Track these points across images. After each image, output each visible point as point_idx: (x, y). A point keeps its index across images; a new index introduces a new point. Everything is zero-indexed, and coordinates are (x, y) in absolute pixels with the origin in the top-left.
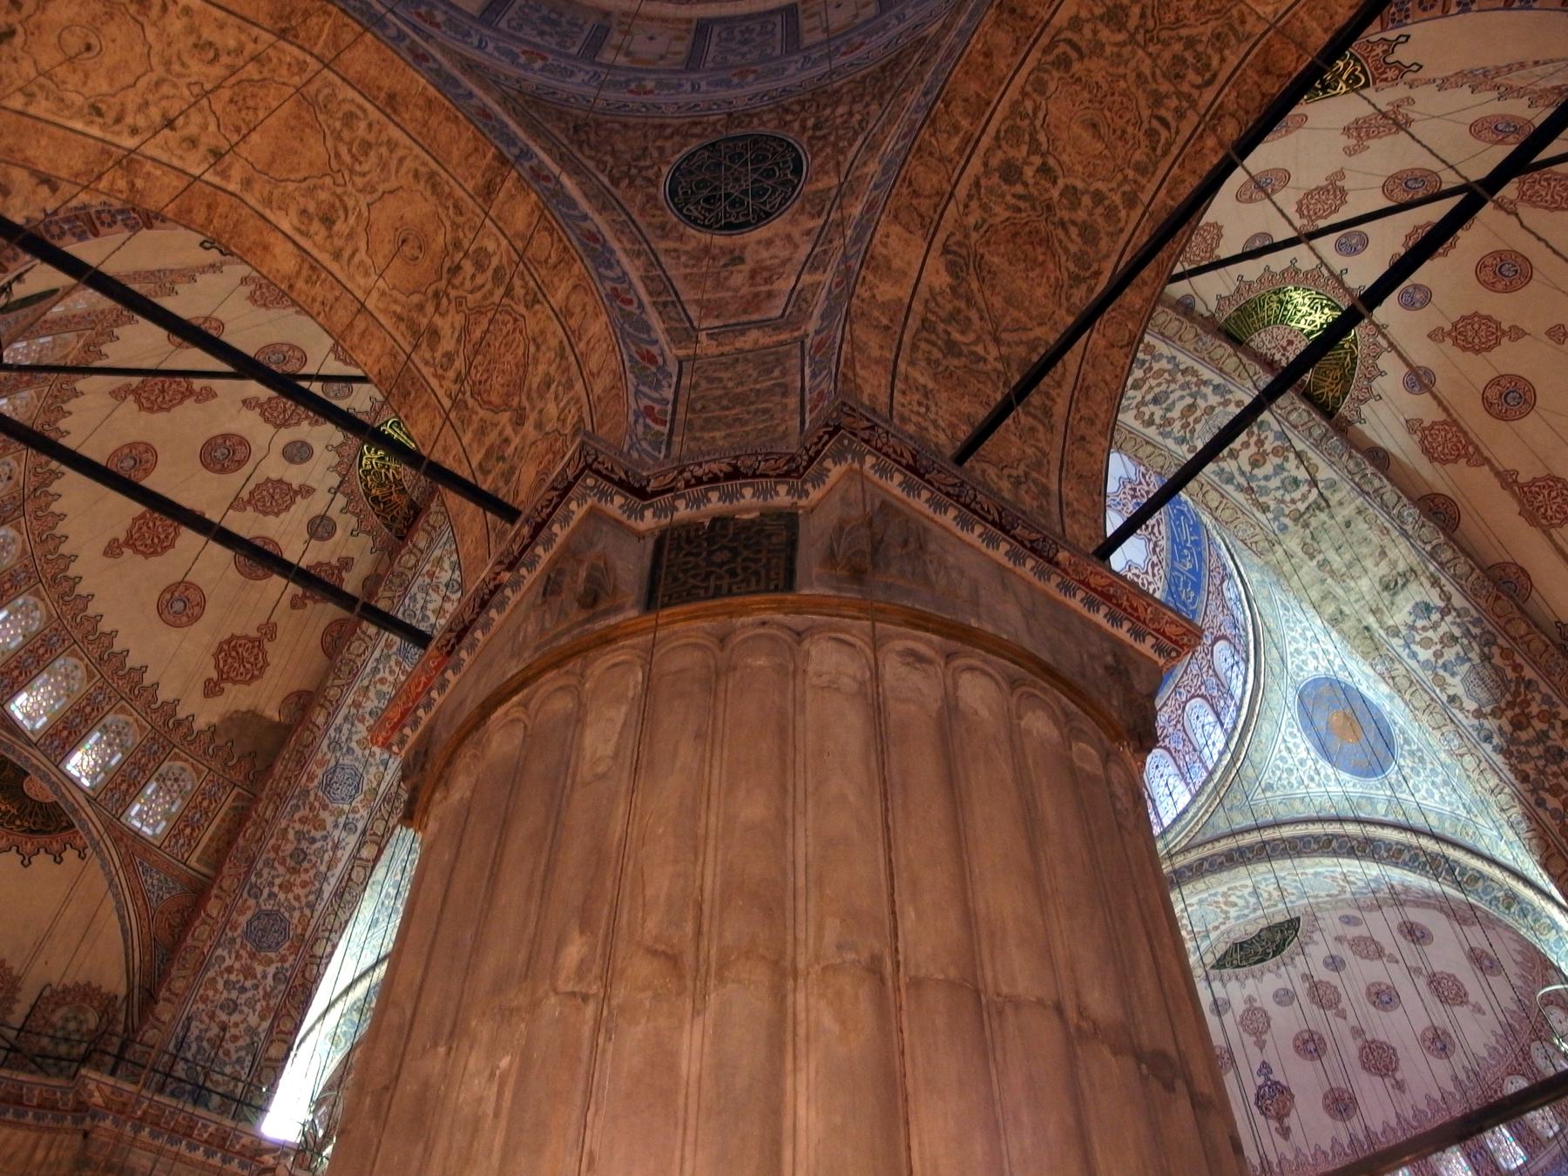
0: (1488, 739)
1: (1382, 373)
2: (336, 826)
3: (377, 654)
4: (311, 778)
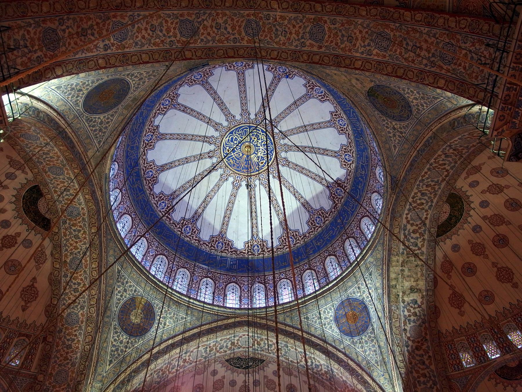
0: (407, 346)
1: (451, 239)
2: (103, 41)
3: (175, 12)
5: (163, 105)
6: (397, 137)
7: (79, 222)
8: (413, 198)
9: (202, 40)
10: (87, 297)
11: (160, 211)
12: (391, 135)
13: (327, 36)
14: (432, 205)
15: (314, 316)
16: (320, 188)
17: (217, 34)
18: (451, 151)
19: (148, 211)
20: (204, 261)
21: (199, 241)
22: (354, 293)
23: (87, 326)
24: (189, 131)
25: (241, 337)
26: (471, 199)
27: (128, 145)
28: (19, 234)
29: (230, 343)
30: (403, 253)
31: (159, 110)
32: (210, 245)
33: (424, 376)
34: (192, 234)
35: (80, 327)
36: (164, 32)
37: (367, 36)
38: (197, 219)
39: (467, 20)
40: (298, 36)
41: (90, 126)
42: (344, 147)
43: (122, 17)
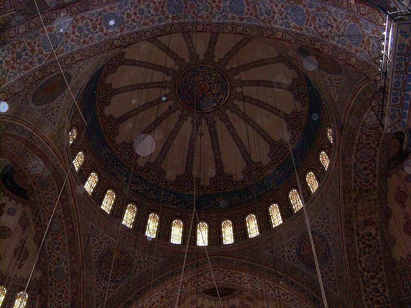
2: (37, 56)
3: (98, 10)
7: (50, 191)
9: (128, 27)
12: (329, 84)
13: (246, 9)
15: (278, 250)
19: (114, 162)
20: (173, 201)
23: (72, 279)
30: (355, 190)
31: (108, 70)
34: (158, 177)
37: (283, 9)
38: (161, 162)
39: (365, 8)
40: (219, 10)
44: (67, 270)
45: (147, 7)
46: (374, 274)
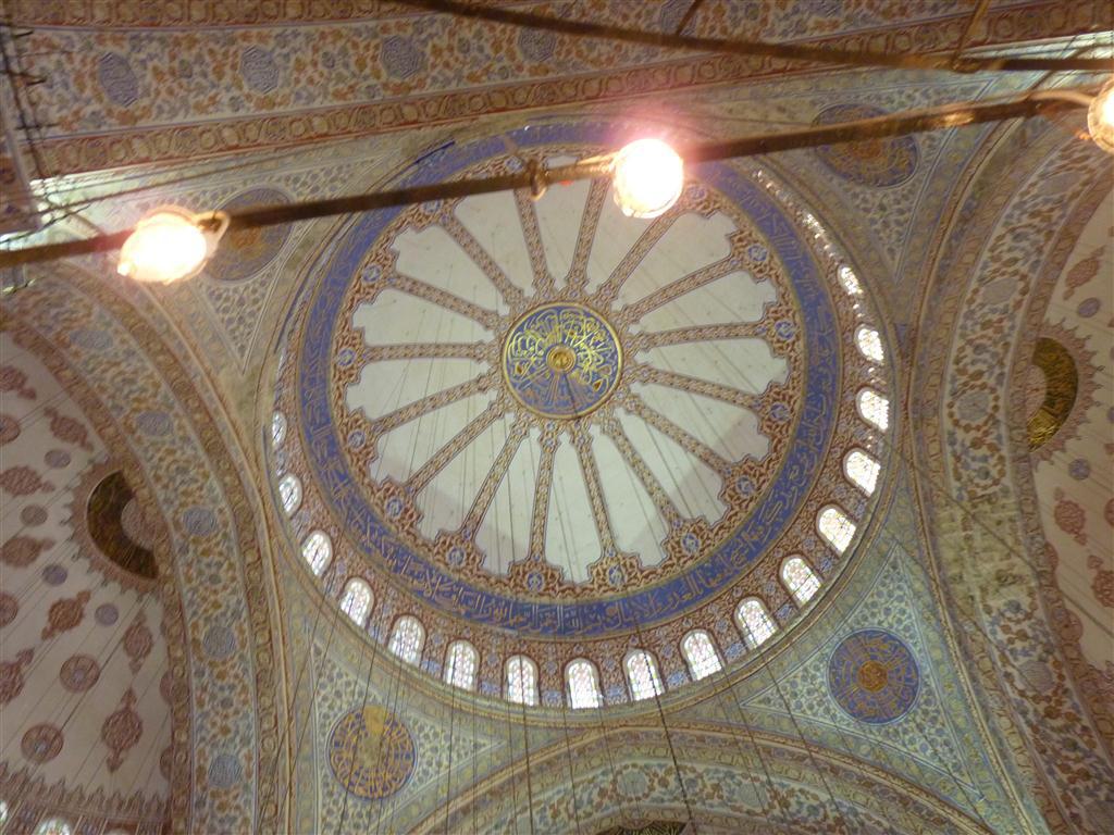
0: (1024, 713)
4: (245, 37)
5: (366, 279)
6: (893, 225)
7: (217, 544)
8: (957, 362)
9: (435, 80)
10: (252, 715)
11: (391, 521)
12: (878, 226)
14: (1002, 374)
16: (736, 413)
17: (464, 64)
18: (1025, 220)
21: (488, 579)
22: (866, 619)
24: (428, 337)
25: (620, 772)
26: (1089, 346)
27: (303, 376)
28: (85, 596)
29: (596, 791)
31: (358, 291)
32: (512, 584)
33: (1087, 776)
35: (246, 787)
36: (353, 68)
38: (474, 531)
41: (217, 310)
42: (773, 309)
43: (262, 38)
44: (249, 758)
45: (474, 37)
46: (1053, 704)
